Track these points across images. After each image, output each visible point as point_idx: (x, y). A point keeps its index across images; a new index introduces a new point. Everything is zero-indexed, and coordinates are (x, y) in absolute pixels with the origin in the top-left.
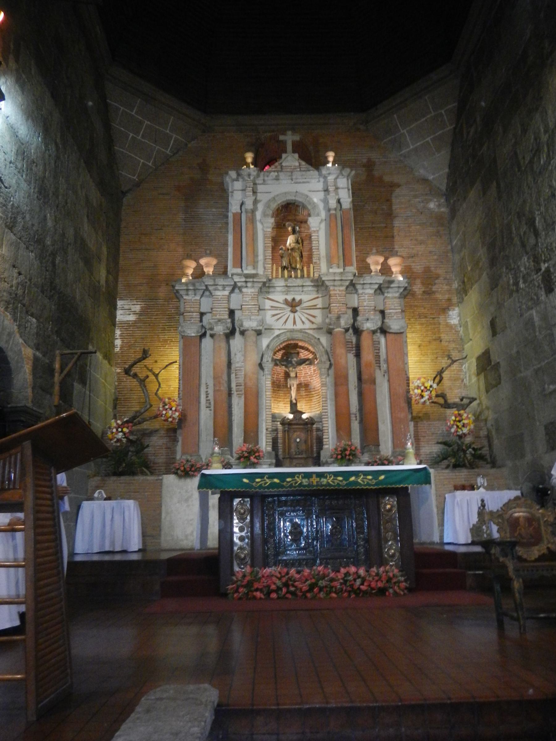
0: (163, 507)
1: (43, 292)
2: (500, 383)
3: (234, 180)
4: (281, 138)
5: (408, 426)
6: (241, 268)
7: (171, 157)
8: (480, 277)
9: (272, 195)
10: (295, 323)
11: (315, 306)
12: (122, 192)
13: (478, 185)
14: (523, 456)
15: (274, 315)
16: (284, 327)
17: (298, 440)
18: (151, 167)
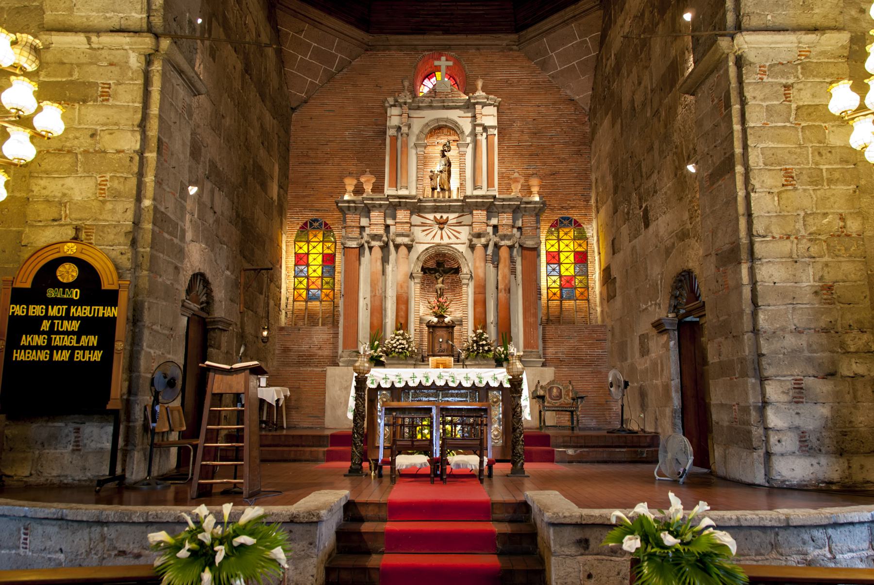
0: (327, 395)
1: (231, 222)
2: (615, 296)
3: (391, 106)
4: (436, 63)
5: (537, 329)
6: (396, 187)
7: (336, 74)
8: (607, 200)
9: (426, 121)
10: (442, 238)
11: (460, 223)
12: (292, 108)
13: (609, 116)
14: (626, 360)
15: (424, 231)
16: (432, 241)
17: (441, 340)
18: (318, 85)
